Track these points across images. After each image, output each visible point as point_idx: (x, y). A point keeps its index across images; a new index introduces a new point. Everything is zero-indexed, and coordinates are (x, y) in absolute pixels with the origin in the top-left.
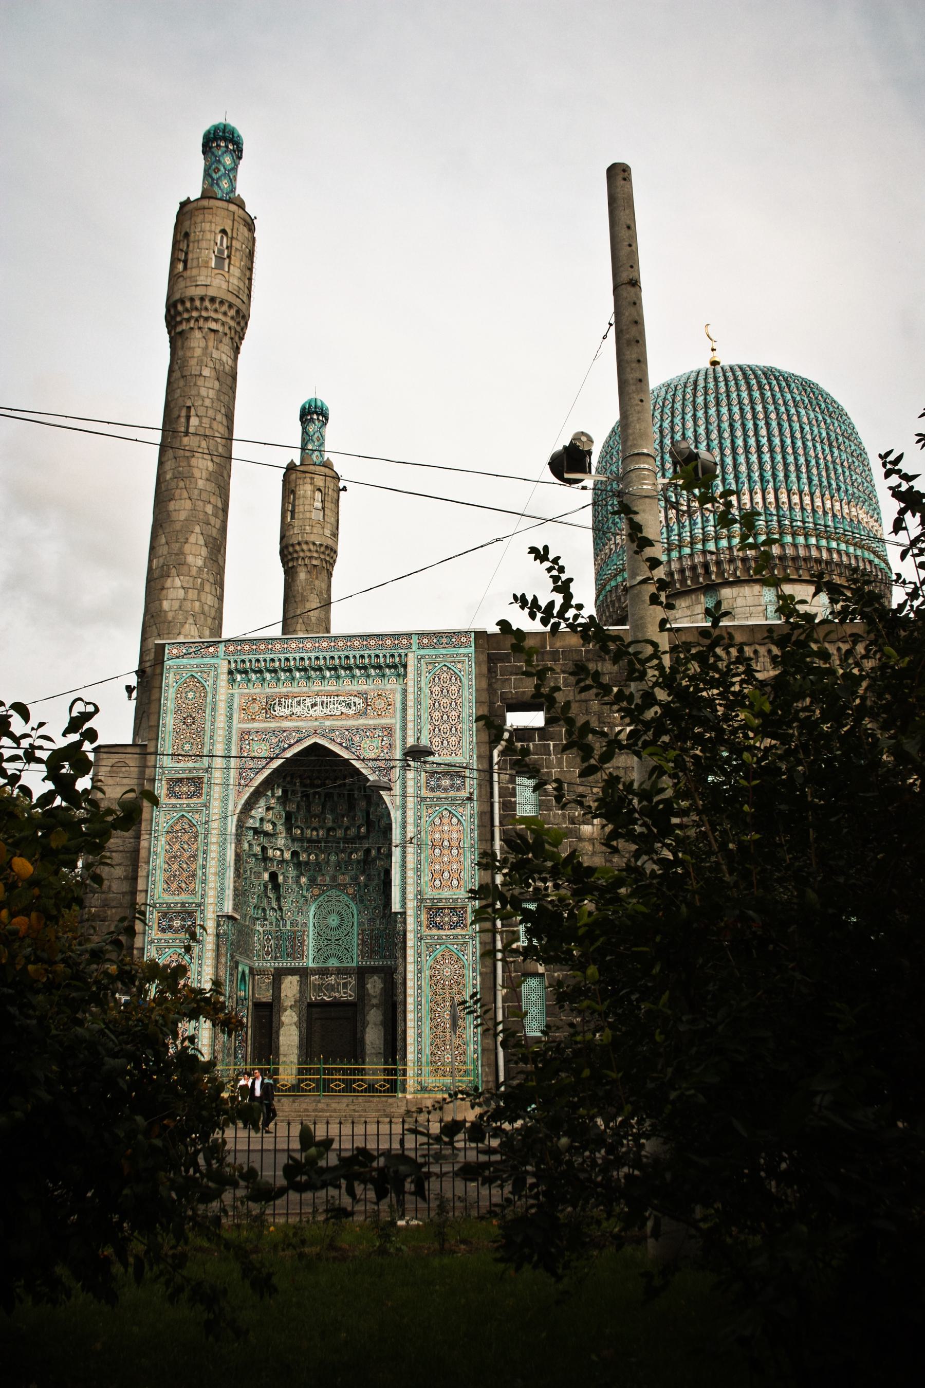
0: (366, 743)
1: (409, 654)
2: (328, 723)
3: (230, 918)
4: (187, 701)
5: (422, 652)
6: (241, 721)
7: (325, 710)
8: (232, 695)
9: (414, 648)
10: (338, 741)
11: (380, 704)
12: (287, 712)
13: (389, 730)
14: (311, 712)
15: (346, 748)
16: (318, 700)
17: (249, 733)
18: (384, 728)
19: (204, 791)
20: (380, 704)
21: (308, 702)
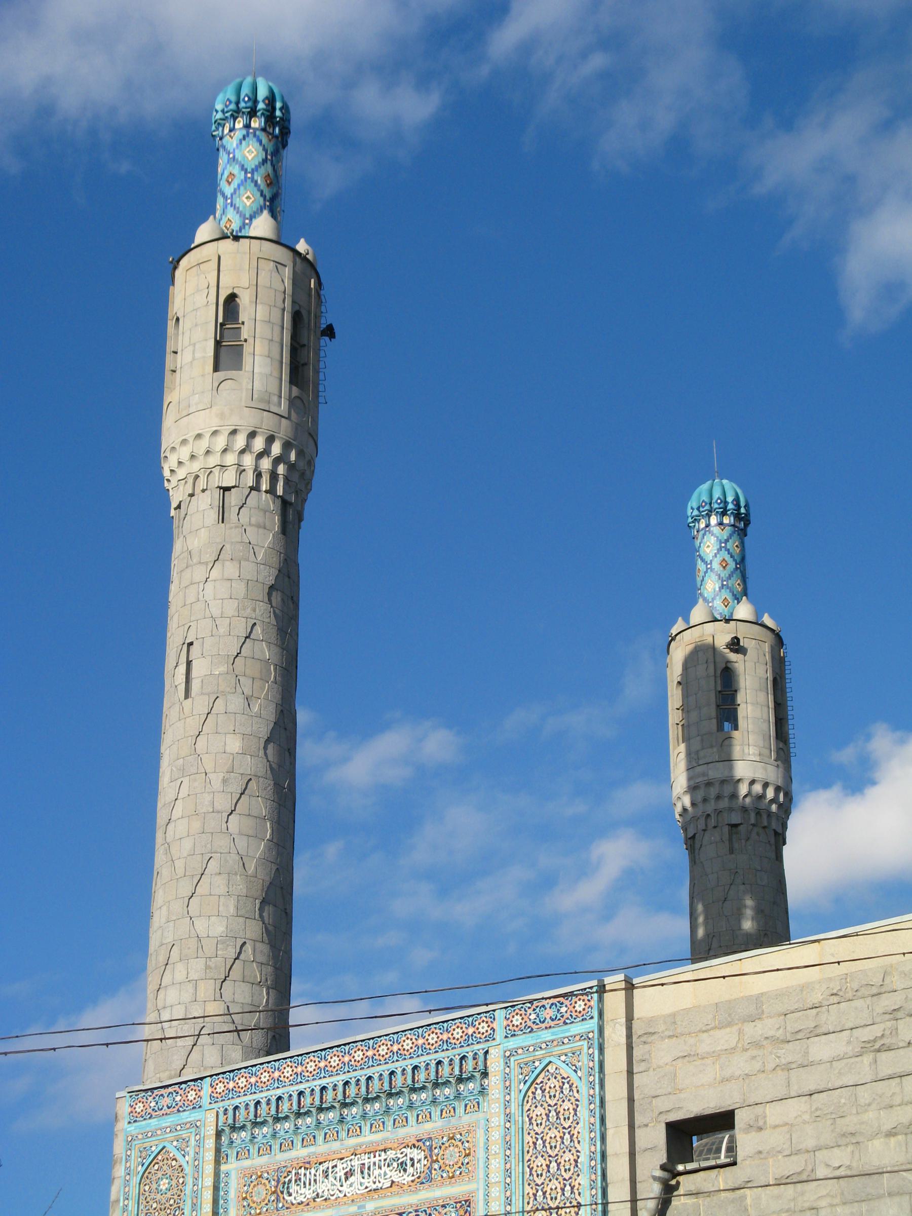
1: (491, 1051)
4: (158, 1197)
5: (512, 1043)
7: (365, 1181)
9: (499, 1035)
11: (452, 1155)
12: (308, 1193)
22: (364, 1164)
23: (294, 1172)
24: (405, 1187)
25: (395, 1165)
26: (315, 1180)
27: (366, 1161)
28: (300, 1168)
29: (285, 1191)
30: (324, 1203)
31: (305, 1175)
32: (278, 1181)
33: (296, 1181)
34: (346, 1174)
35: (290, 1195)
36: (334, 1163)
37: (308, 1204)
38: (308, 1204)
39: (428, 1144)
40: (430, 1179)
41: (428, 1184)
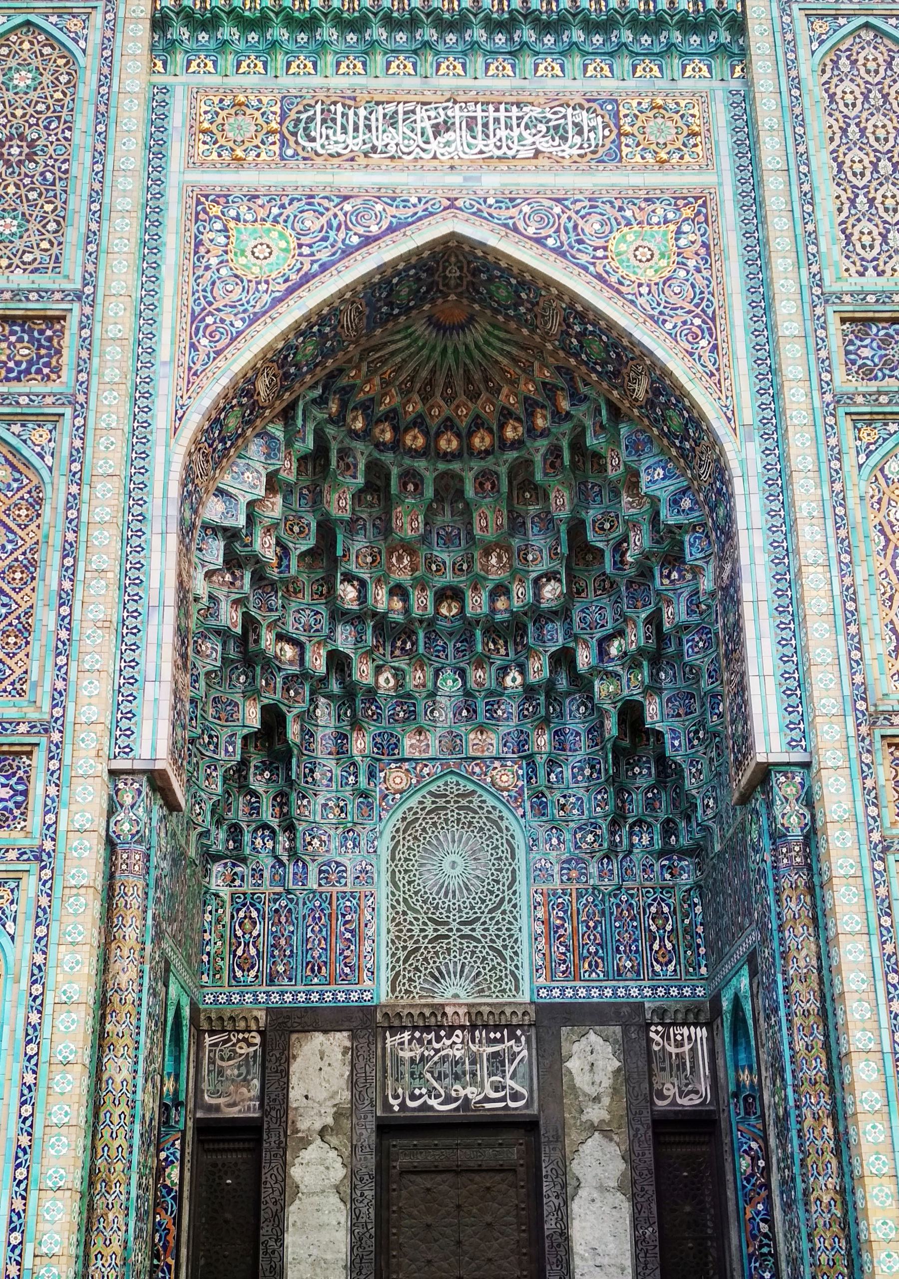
0: (623, 242)
2: (492, 181)
3: (157, 782)
6: (192, 164)
7: (480, 143)
8: (165, 90)
10: (531, 231)
12: (355, 143)
13: (700, 206)
14: (434, 146)
15: (559, 252)
16: (456, 113)
17: (224, 198)
18: (679, 199)
19: (68, 358)
20: (660, 130)
21: (423, 119)
22: (475, 118)
23: (319, 107)
24: (566, 163)
25: (542, 127)
26: (368, 127)
27: (479, 114)
28: (335, 103)
29: (301, 132)
30: (388, 162)
31: (343, 114)
32: (283, 116)
33: (324, 121)
34: (436, 126)
35: (313, 140)
36: (409, 106)
37: (352, 159)
38: (352, 159)
39: (610, 107)
40: (615, 156)
41: (614, 163)
